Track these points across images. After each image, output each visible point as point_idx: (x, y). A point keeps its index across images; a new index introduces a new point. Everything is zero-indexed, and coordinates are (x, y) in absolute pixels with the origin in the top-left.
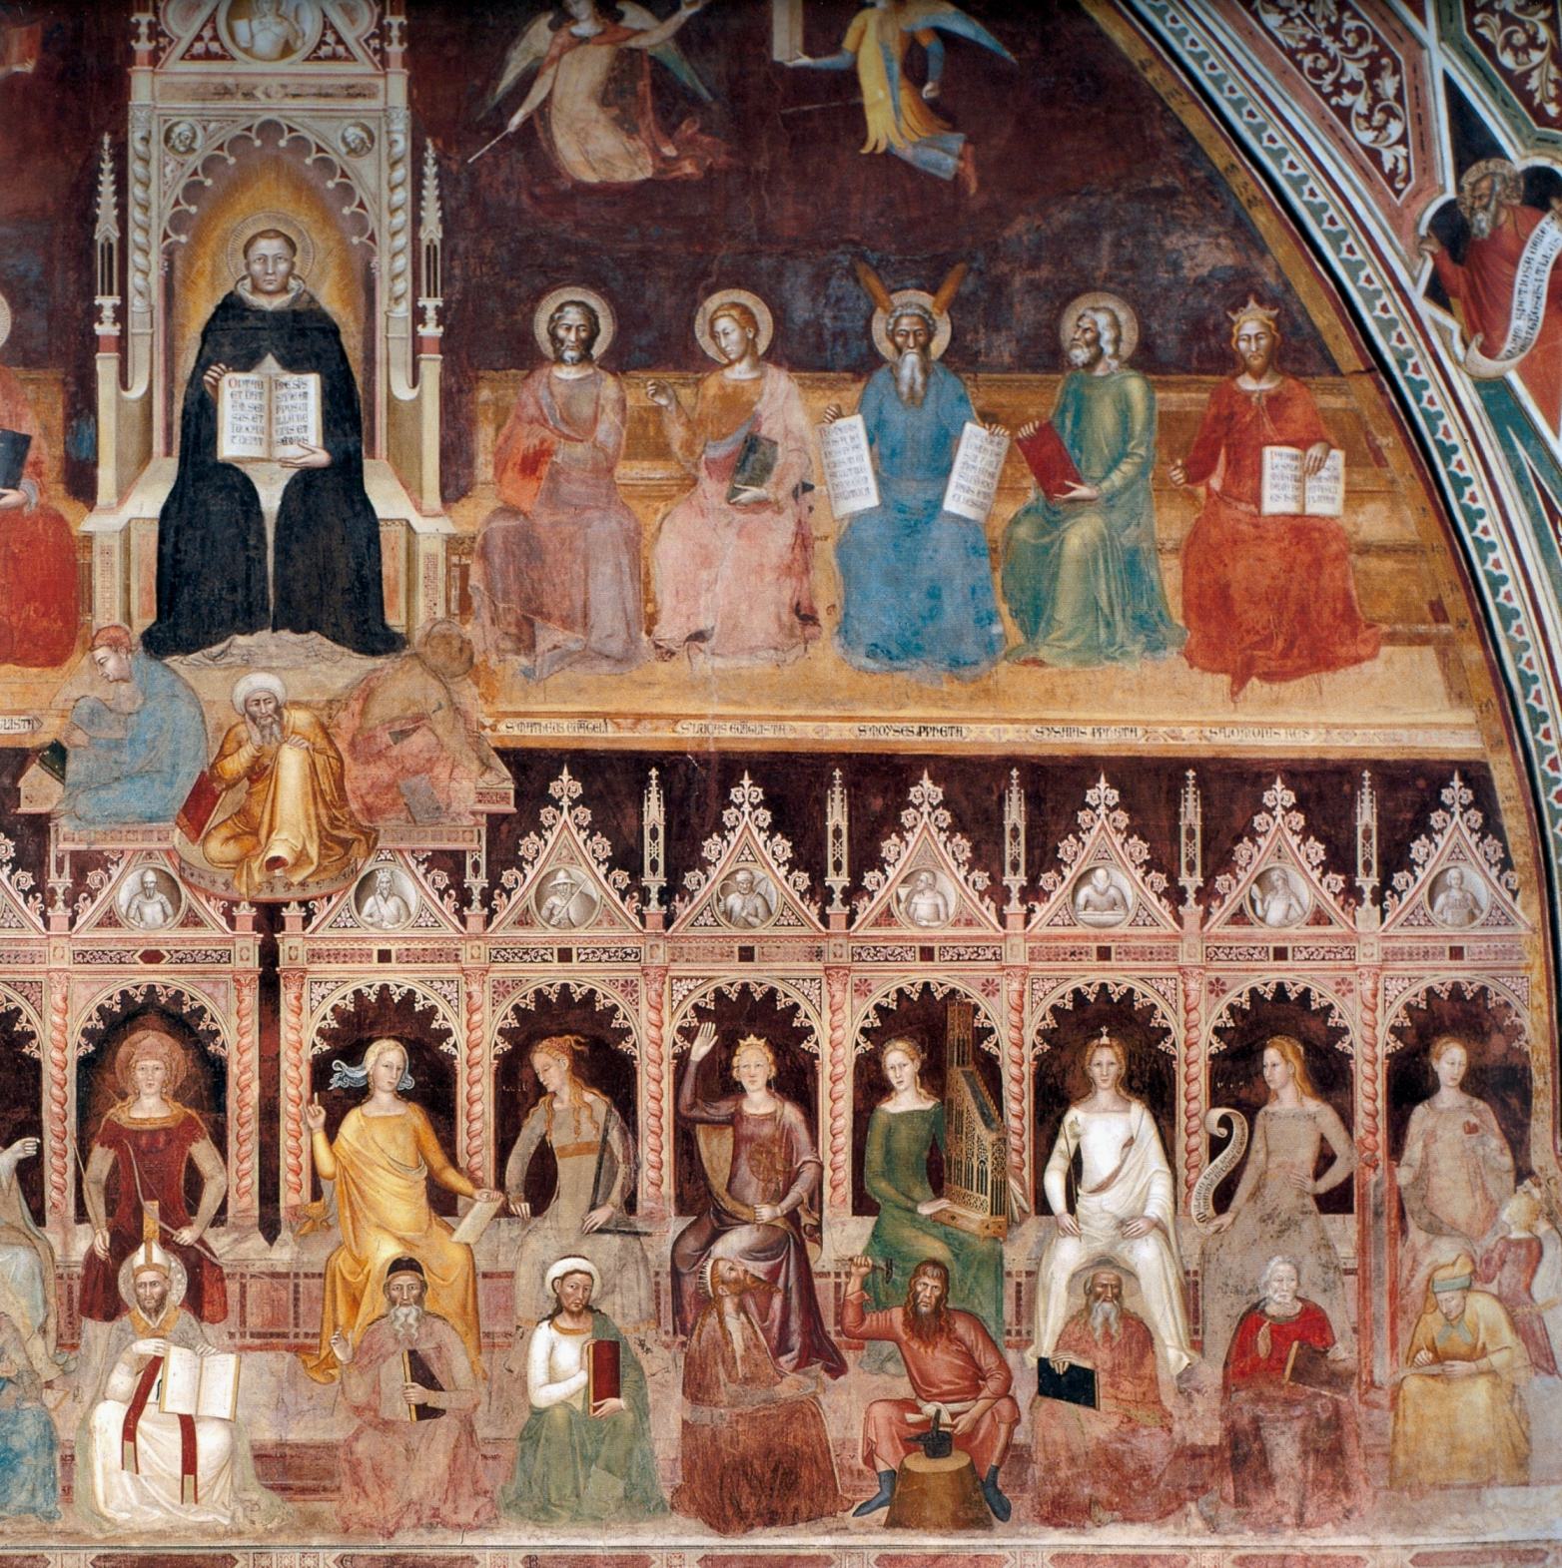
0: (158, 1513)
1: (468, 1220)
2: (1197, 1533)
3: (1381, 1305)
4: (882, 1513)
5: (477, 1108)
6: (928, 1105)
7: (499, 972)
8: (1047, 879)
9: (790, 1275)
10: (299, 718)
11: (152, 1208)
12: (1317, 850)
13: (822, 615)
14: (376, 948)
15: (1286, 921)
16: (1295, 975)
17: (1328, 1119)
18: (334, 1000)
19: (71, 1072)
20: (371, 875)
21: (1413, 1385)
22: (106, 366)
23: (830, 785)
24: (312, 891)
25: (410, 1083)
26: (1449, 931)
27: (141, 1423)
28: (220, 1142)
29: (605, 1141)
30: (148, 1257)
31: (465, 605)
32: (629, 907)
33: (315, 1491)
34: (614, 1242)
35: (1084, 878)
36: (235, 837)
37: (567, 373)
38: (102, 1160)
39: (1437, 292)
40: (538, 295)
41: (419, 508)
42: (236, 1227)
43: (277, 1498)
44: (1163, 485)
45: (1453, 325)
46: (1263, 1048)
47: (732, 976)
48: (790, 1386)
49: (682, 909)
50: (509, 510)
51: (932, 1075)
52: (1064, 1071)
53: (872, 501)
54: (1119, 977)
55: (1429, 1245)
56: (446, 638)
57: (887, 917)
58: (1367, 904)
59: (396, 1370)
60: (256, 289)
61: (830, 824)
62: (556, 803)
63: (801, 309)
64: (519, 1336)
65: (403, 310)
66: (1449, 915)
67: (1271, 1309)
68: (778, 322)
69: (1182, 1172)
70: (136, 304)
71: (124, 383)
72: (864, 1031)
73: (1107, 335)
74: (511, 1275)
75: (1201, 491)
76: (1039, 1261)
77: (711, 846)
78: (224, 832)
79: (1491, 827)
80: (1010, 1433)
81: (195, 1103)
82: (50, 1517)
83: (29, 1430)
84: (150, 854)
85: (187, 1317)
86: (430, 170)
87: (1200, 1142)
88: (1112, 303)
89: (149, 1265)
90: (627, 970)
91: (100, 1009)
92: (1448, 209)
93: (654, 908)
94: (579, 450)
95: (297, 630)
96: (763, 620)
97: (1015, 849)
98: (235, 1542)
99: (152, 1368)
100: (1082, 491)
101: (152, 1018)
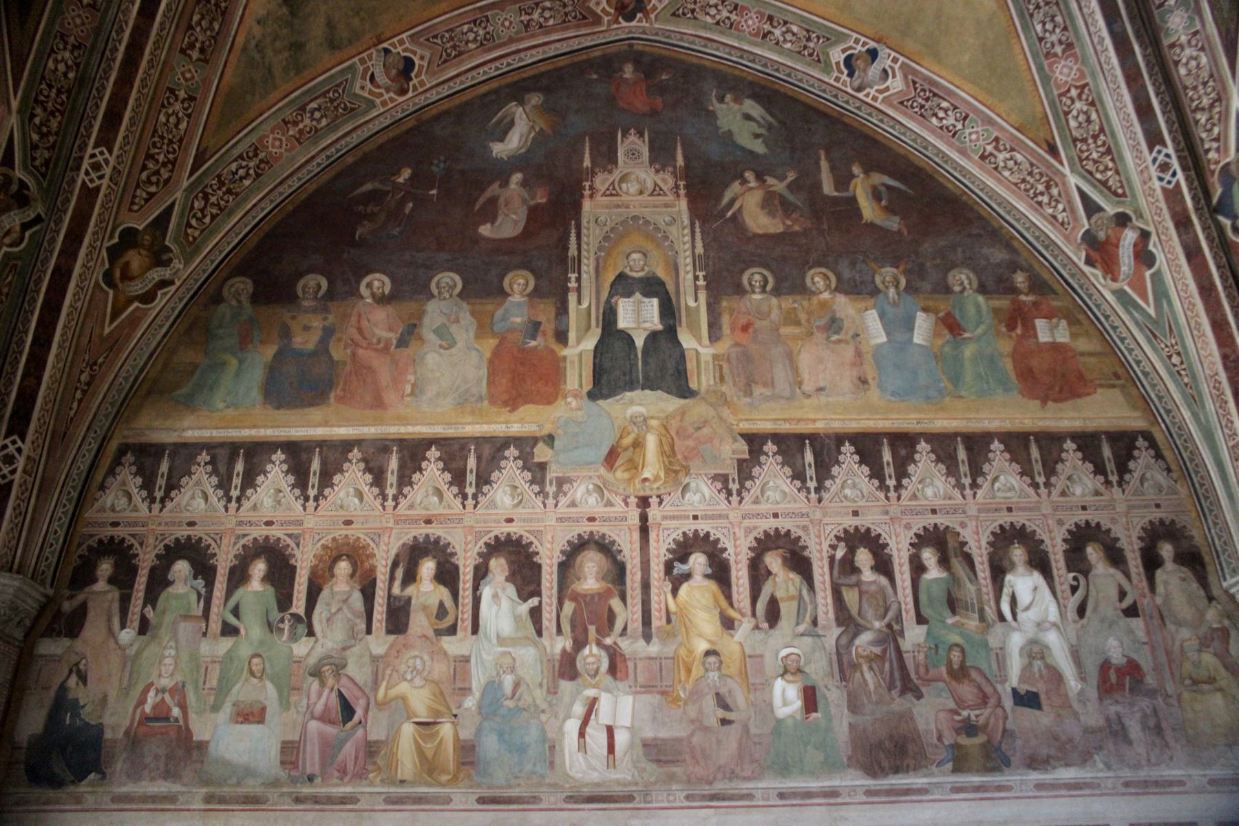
0: (596, 774)
1: (740, 631)
2: (1101, 771)
3: (1163, 658)
4: (949, 766)
5: (741, 581)
6: (944, 575)
7: (747, 523)
8: (980, 480)
9: (891, 652)
10: (654, 423)
11: (592, 629)
12: (1090, 467)
13: (870, 381)
14: (691, 514)
15: (1083, 495)
16: (1092, 516)
17: (1120, 576)
18: (674, 536)
19: (555, 568)
20: (688, 484)
21: (1186, 695)
22: (572, 298)
23: (882, 444)
24: (662, 491)
25: (709, 571)
26: (1152, 497)
27: (588, 730)
28: (623, 598)
29: (801, 597)
30: (591, 651)
31: (722, 379)
32: (802, 495)
33: (672, 762)
34: (808, 640)
35: (996, 479)
36: (627, 470)
37: (757, 297)
38: (569, 607)
39: (1089, 262)
40: (742, 271)
41: (700, 344)
42: (631, 637)
43: (654, 766)
44: (998, 333)
45: (1098, 273)
46: (1084, 547)
47: (850, 523)
48: (899, 704)
49: (825, 495)
50: (737, 344)
51: (944, 562)
52: (1001, 560)
53: (884, 339)
54: (1019, 519)
55: (1177, 631)
56: (715, 392)
57: (914, 497)
58: (1116, 487)
59: (709, 702)
60: (631, 270)
61: (885, 460)
62: (767, 454)
63: (847, 274)
64: (767, 685)
65: (690, 276)
66: (1151, 491)
67: (1114, 661)
68: (839, 278)
69: (1061, 601)
70: (584, 276)
71: (579, 302)
72: (911, 544)
73: (966, 282)
74: (761, 656)
75: (1013, 334)
76: (1004, 642)
77: (835, 470)
78: (623, 468)
79: (1159, 456)
80: (1004, 724)
81: (613, 582)
82: (543, 776)
83: (533, 734)
84: (590, 478)
85: (609, 679)
86: (698, 230)
87: (1067, 587)
88: (966, 271)
89: (591, 655)
90: (805, 522)
91: (568, 542)
92: (1087, 232)
93: (813, 495)
94: (765, 323)
95: (652, 389)
96: (846, 381)
97: (964, 468)
98: (634, 788)
99: (592, 705)
100: (967, 335)
101: (592, 546)
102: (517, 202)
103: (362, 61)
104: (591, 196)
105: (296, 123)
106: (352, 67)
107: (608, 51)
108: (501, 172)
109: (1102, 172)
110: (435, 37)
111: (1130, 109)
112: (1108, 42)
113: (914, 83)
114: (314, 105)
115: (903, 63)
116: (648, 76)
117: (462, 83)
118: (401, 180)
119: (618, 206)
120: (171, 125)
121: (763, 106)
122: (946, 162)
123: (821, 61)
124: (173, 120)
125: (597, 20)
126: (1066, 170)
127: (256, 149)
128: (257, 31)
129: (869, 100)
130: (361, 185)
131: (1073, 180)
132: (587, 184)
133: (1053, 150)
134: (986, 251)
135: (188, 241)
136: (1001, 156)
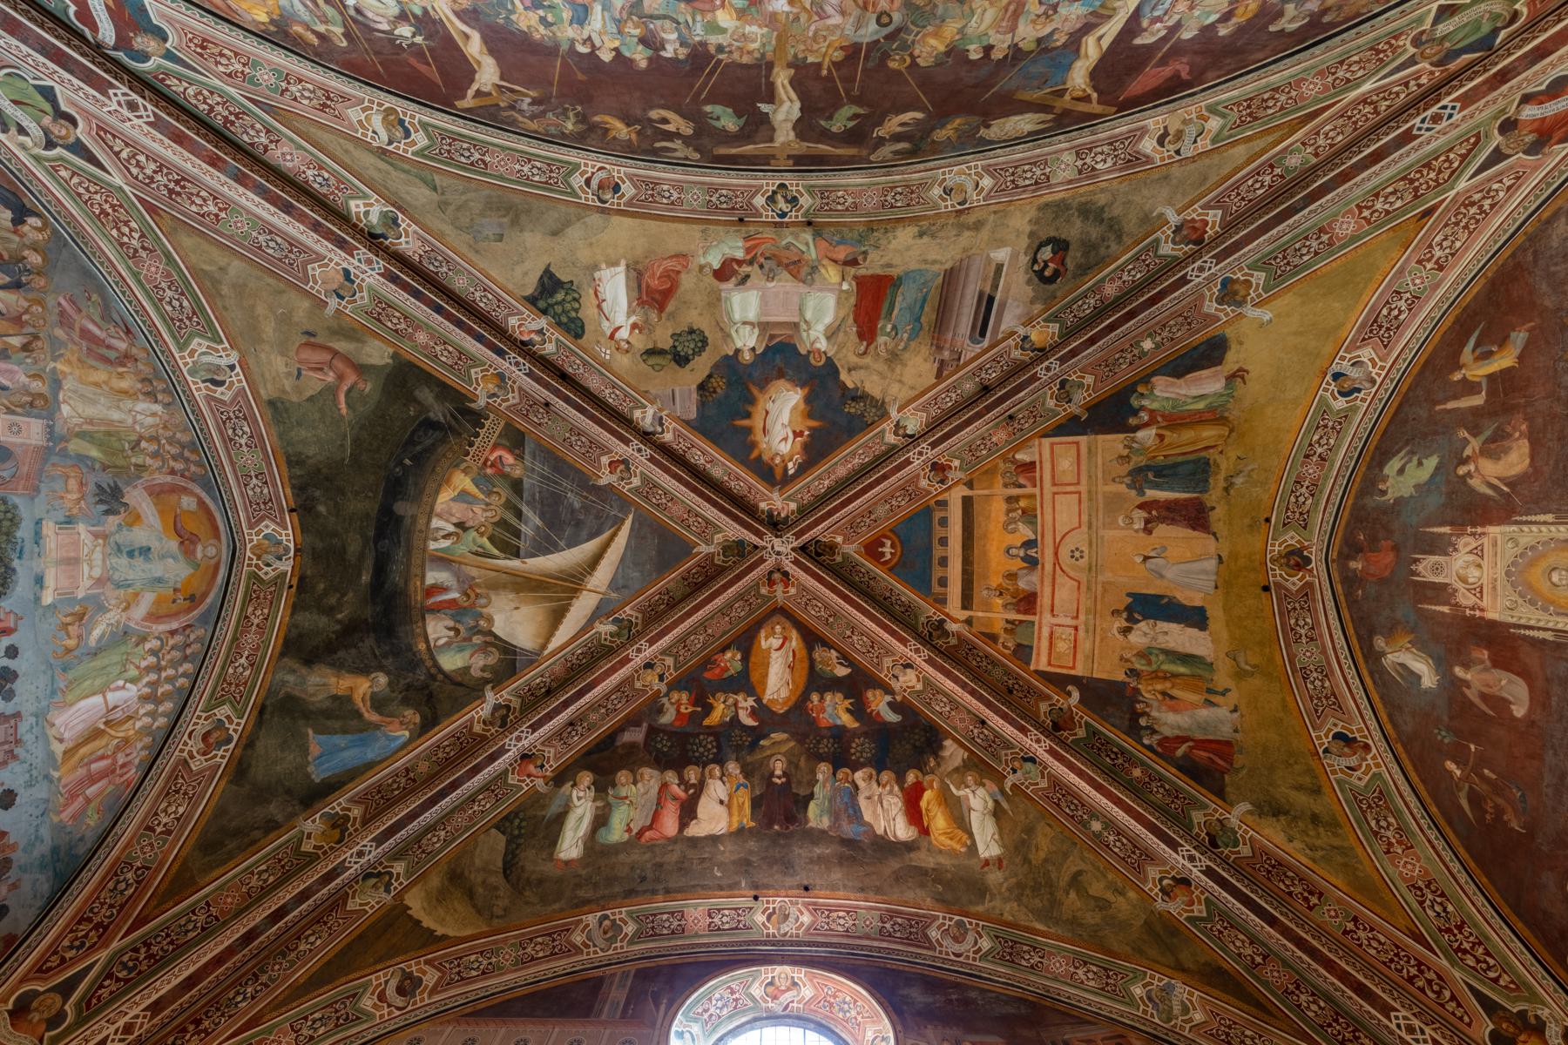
86: (1524, 518)
92: (1525, 153)
102: (1486, 676)
103: (1334, 772)
104: (1482, 610)
105: (1390, 844)
106: (1338, 782)
107: (1338, 579)
108: (1453, 687)
109: (1451, 163)
110: (1316, 711)
111: (1377, 167)
112: (1312, 207)
113: (1364, 339)
114: (1373, 823)
115: (1345, 351)
116: (1361, 550)
117: (1361, 698)
118: (1458, 773)
119: (1494, 588)
120: (1380, 948)
121: (1390, 459)
122: (1448, 299)
123: (1346, 416)
124: (1375, 944)
125: (1310, 585)
126: (1452, 193)
127: (1413, 886)
128: (1297, 844)
129: (1384, 373)
130: (1460, 808)
131: (1462, 185)
132: (1468, 612)
133: (1428, 213)
134: (1555, 244)
135: (1512, 990)
136: (1438, 253)
